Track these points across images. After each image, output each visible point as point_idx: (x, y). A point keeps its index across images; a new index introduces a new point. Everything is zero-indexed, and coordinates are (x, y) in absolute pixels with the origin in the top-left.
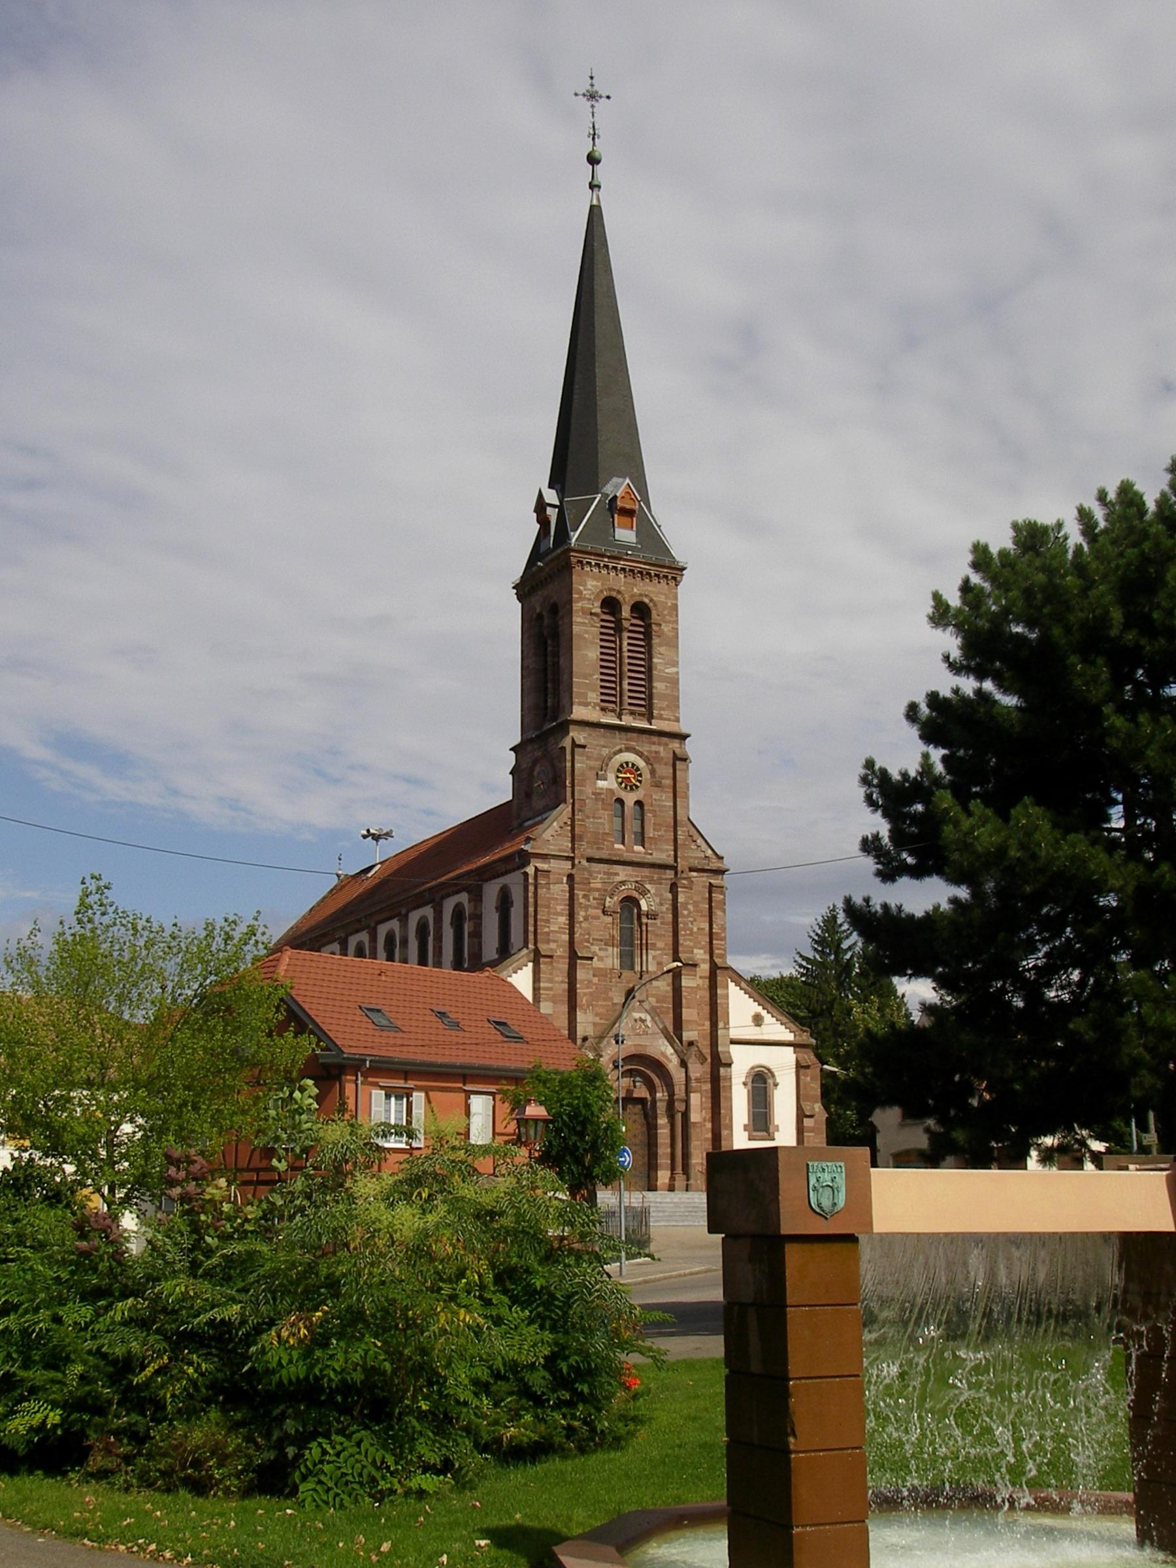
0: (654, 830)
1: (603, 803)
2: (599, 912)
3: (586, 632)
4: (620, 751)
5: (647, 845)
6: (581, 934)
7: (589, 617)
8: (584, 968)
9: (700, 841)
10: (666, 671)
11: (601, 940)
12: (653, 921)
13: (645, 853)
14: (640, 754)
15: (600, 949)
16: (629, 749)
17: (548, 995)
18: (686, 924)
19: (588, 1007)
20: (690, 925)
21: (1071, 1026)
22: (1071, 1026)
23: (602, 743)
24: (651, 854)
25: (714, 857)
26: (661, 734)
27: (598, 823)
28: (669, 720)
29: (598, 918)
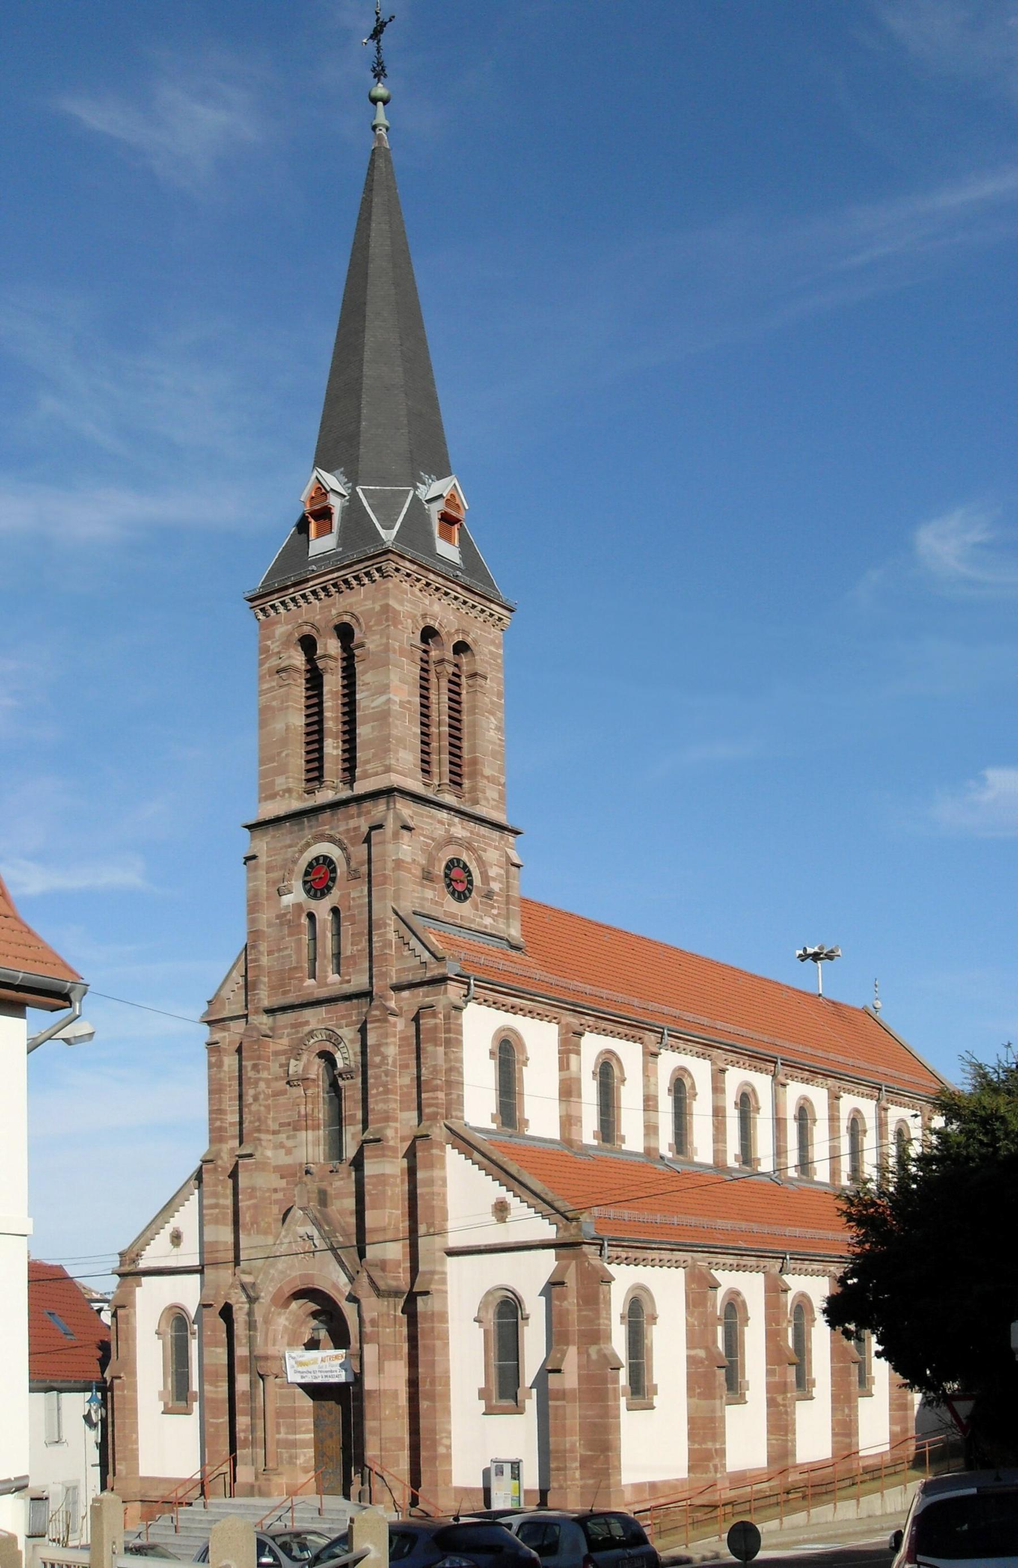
0: (352, 944)
1: (290, 927)
2: (281, 1084)
3: (274, 698)
4: (308, 845)
5: (343, 970)
6: (250, 1122)
7: (277, 676)
8: (246, 1171)
9: (414, 942)
10: (373, 705)
11: (289, 1124)
12: (351, 1081)
13: (341, 983)
14: (332, 840)
15: (288, 1138)
16: (320, 838)
17: (212, 1215)
18: (377, 1077)
19: (252, 1224)
20: (384, 1078)
21: (790, 1480)
22: (790, 1480)
23: (288, 842)
24: (349, 981)
25: (433, 960)
26: (374, 796)
27: (283, 957)
28: (376, 774)
29: (284, 1092)
